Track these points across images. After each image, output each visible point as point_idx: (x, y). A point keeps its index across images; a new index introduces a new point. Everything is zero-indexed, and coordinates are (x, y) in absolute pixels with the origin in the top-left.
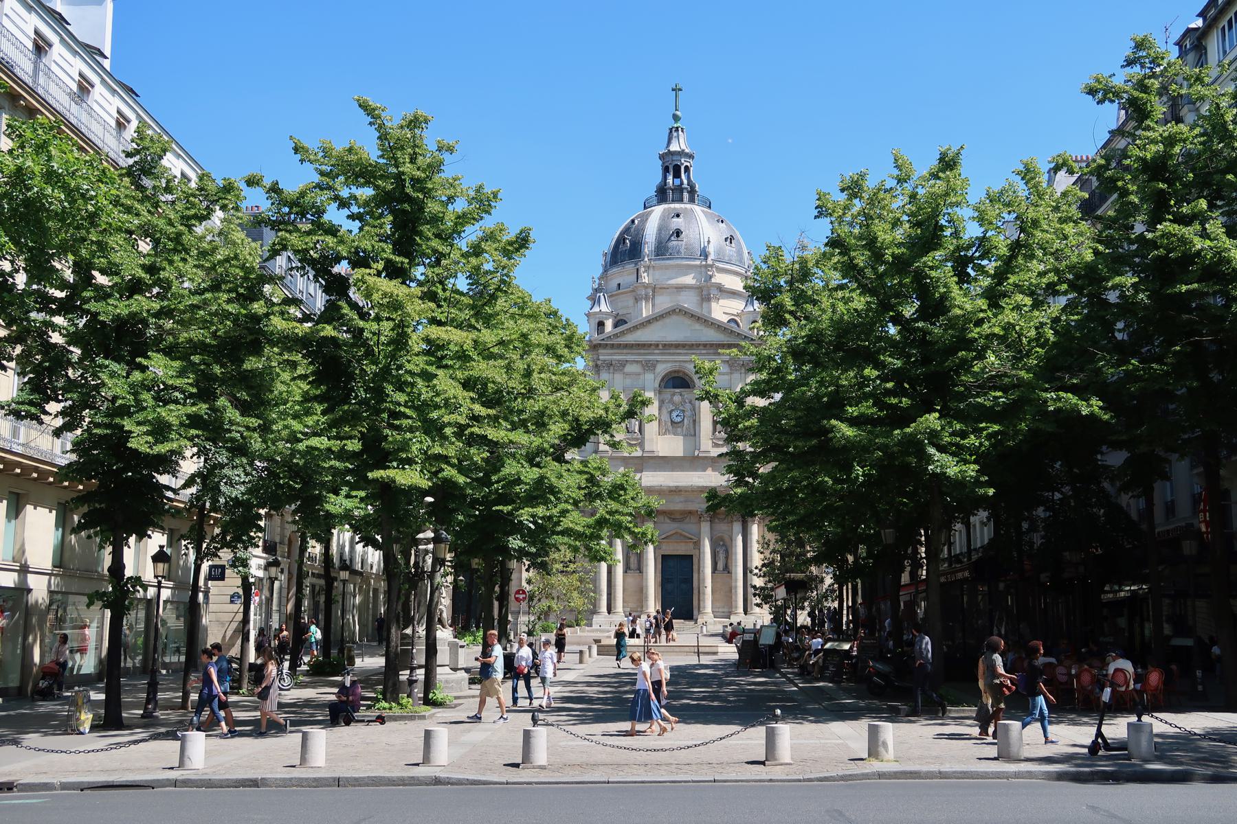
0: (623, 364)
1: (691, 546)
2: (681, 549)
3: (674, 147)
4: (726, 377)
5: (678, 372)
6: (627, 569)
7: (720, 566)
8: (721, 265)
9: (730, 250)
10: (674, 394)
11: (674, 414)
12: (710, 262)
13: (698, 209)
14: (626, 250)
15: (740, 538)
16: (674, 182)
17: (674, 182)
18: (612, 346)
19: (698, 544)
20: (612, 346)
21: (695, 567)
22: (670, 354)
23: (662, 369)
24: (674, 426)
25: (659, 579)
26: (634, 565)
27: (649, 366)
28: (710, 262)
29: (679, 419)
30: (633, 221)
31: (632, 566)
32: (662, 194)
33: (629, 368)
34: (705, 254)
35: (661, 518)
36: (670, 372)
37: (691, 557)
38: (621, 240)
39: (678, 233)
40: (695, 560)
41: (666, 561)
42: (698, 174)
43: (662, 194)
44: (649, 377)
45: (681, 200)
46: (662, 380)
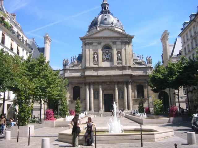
0: (92, 43)
1: (112, 91)
2: (109, 92)
3: (104, 3)
4: (120, 46)
5: (107, 45)
6: (94, 98)
7: (121, 96)
8: (116, 26)
9: (118, 24)
10: (106, 51)
11: (106, 56)
12: (114, 25)
13: (110, 15)
14: (94, 24)
15: (126, 88)
16: (105, 9)
17: (105, 9)
18: (89, 38)
19: (114, 90)
20: (89, 38)
21: (114, 97)
22: (105, 40)
23: (103, 44)
24: (107, 60)
25: (104, 101)
26: (97, 96)
27: (99, 43)
28: (114, 25)
29: (108, 57)
30: (95, 18)
31: (96, 98)
32: (102, 13)
33: (94, 44)
34: (112, 23)
35: (103, 84)
36: (105, 45)
37: (112, 95)
38: (93, 22)
39: (106, 19)
40: (113, 95)
41: (105, 96)
42: (110, 8)
43: (102, 13)
44: (99, 46)
45: (106, 13)
46: (103, 47)
